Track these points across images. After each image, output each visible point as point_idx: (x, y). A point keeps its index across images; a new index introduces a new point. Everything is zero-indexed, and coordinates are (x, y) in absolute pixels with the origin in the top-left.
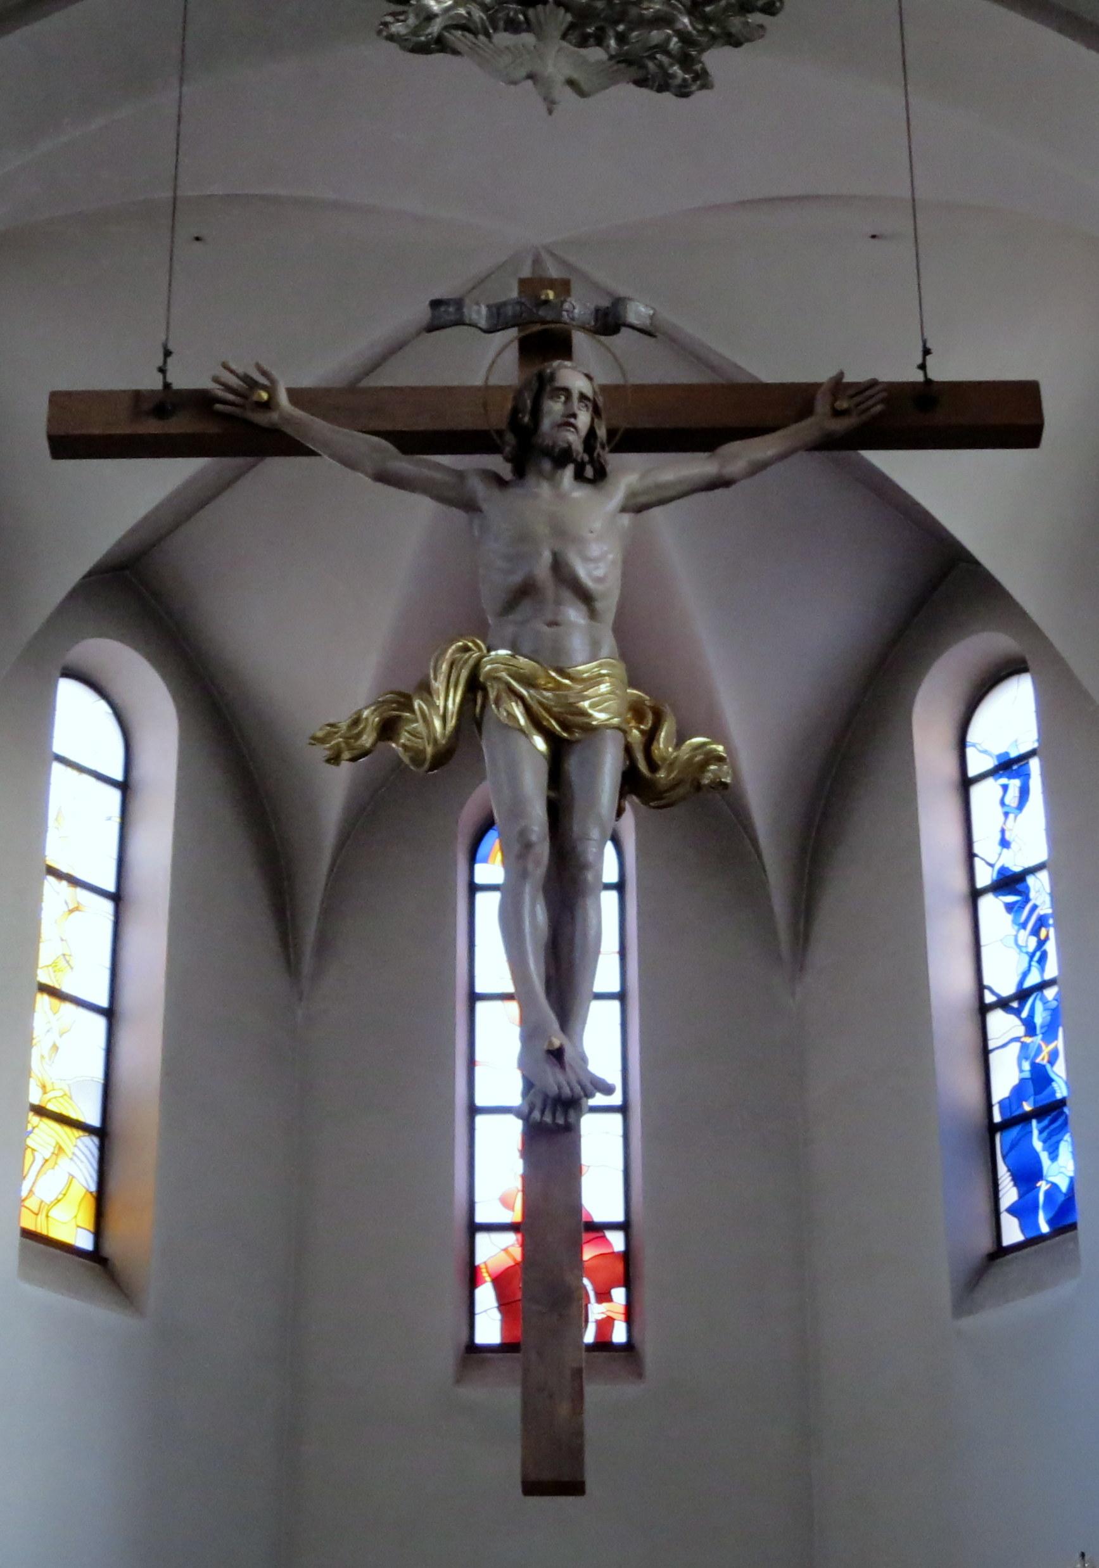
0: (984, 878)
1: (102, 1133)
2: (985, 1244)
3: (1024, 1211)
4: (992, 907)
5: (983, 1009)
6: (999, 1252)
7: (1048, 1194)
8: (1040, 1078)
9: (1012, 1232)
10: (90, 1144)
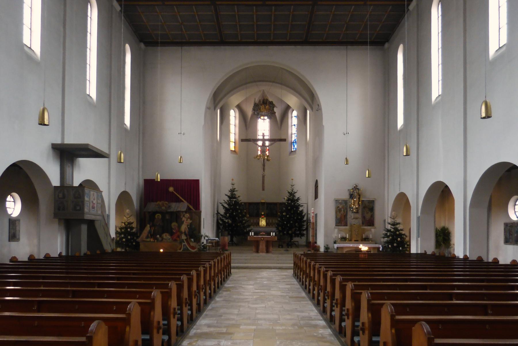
0: (293, 125)
1: (235, 142)
2: (291, 151)
3: (294, 148)
4: (293, 127)
5: (292, 134)
6: (292, 151)
7: (295, 148)
8: (295, 140)
9: (293, 150)
10: (234, 143)
